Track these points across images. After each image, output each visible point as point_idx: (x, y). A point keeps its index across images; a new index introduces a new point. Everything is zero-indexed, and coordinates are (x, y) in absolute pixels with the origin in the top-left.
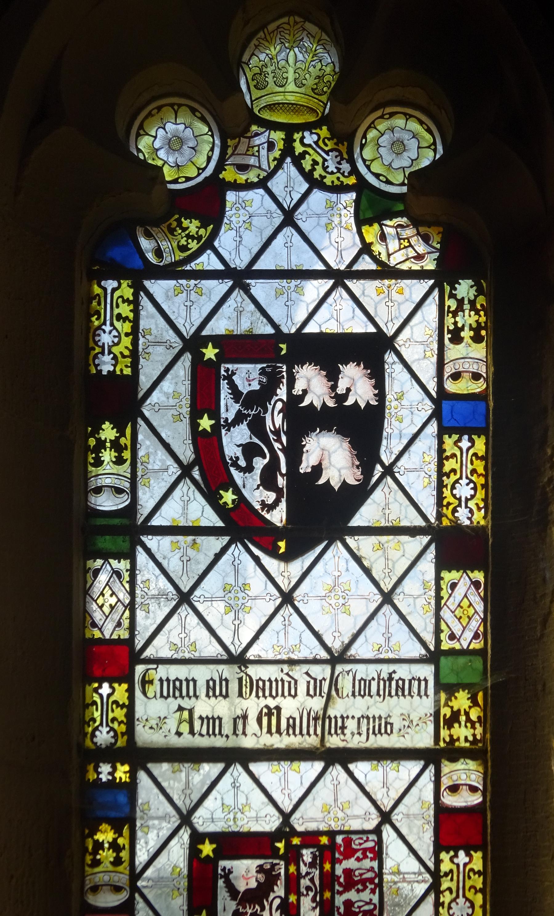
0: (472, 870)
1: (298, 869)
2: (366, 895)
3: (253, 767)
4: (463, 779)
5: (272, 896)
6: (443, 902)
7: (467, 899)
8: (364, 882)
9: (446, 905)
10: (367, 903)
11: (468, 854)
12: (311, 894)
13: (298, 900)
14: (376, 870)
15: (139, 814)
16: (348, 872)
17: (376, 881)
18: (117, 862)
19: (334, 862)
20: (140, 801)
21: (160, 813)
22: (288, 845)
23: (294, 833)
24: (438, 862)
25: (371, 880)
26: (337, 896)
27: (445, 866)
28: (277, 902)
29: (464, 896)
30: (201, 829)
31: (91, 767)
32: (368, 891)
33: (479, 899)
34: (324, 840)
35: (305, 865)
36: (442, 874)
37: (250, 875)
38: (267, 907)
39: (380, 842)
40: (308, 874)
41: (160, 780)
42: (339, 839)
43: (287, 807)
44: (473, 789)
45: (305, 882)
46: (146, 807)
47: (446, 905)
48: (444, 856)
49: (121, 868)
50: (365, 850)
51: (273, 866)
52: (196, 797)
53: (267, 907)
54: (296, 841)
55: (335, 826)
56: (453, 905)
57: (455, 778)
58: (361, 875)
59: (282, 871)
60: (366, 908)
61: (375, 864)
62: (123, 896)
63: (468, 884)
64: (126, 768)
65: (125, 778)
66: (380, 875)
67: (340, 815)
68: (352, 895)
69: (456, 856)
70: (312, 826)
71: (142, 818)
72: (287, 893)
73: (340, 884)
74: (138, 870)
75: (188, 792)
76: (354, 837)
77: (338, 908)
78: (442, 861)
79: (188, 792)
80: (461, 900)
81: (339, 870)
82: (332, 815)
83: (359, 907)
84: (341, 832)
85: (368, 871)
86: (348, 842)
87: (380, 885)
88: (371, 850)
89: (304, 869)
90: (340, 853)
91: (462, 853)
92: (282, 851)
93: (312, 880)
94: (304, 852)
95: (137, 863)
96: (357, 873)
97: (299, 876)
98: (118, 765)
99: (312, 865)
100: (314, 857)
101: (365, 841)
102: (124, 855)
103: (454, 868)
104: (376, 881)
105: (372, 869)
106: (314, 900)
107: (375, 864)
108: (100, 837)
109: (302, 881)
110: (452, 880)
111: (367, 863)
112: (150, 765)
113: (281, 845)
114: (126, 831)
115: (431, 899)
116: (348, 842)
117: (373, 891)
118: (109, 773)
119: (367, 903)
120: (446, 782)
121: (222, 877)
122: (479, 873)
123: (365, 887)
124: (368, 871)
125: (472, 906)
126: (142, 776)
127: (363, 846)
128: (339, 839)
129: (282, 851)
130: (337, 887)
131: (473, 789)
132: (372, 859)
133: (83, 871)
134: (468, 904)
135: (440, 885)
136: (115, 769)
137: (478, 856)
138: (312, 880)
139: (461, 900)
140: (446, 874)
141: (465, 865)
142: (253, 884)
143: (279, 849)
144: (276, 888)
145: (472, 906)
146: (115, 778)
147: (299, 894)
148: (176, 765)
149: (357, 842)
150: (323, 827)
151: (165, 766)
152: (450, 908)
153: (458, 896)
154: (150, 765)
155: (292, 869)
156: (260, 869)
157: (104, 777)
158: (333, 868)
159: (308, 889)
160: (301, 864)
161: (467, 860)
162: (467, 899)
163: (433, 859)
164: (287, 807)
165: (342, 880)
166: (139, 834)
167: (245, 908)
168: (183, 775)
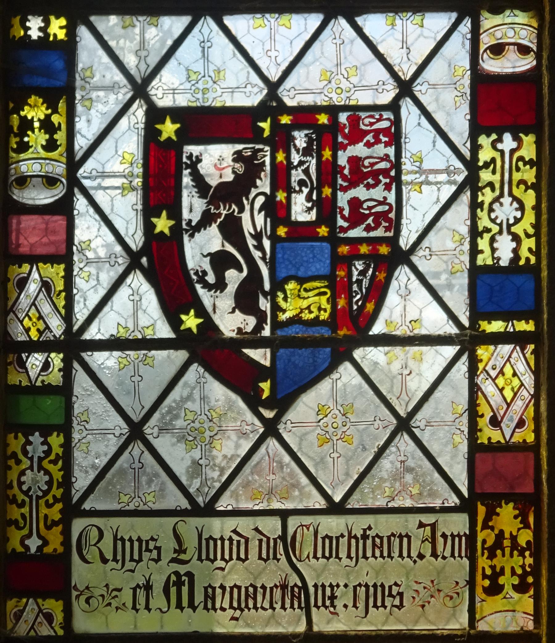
0: (521, 158)
1: (288, 157)
2: (378, 193)
3: (229, 21)
4: (510, 36)
5: (254, 192)
6: (482, 203)
7: (515, 199)
8: (375, 174)
9: (486, 206)
10: (380, 203)
11: (516, 138)
12: (306, 190)
13: (288, 199)
14: (393, 158)
15: (78, 83)
16: (354, 161)
17: (393, 173)
18: (51, 146)
19: (336, 148)
20: (80, 66)
21: (107, 81)
22: (275, 125)
23: (284, 109)
24: (475, 148)
25: (385, 172)
26: (340, 194)
27: (485, 155)
28: (261, 200)
29: (511, 194)
30: (161, 103)
31: (16, 21)
32: (381, 187)
33: (530, 198)
34: (323, 119)
35: (298, 151)
36: (481, 164)
37: (225, 164)
38: (247, 207)
39: (397, 122)
40: (301, 163)
41: (106, 38)
42: (343, 118)
43: (274, 75)
44: (523, 50)
45: (297, 175)
46: (88, 74)
47: (486, 206)
48: (484, 141)
49: (54, 155)
50: (377, 132)
51: (256, 152)
52: (153, 61)
53: (247, 207)
54: (285, 120)
55: (338, 100)
56: (496, 206)
57: (499, 34)
58: (372, 165)
59: (268, 160)
60: (379, 209)
61: (391, 151)
62: (59, 192)
63: (517, 176)
64: (63, 21)
65: (61, 35)
66: (397, 165)
67: (345, 85)
68: (360, 192)
69: (500, 140)
70: (307, 100)
71: (83, 88)
72: (274, 187)
73: (344, 178)
74: (78, 158)
75: (144, 53)
76: (363, 115)
77: (342, 210)
78: (480, 147)
79: (144, 53)
80: (506, 200)
81: (342, 159)
82: (333, 85)
83: (370, 208)
84: (345, 108)
85: (382, 159)
86: (354, 121)
87: (397, 181)
88: (385, 132)
89: (296, 158)
90: (345, 136)
91: (507, 137)
92: (266, 133)
93: (306, 172)
94: (296, 134)
95: (77, 147)
96: (366, 163)
97: (289, 166)
98: (52, 18)
99: (307, 152)
100: (310, 142)
101: (379, 120)
102: (61, 137)
103: (497, 155)
104: (393, 173)
105: (386, 158)
106: (309, 198)
107: (391, 151)
108: (28, 113)
109: (293, 172)
110: (494, 172)
111: (380, 150)
112: (93, 18)
113: (265, 125)
114: (62, 106)
115: (466, 197)
116: (354, 121)
117: (388, 187)
118: (40, 29)
119: (380, 203)
120: (486, 41)
121: (188, 166)
122: (531, 163)
123: (378, 182)
124: (382, 159)
125: (522, 208)
126: (83, 32)
127: (375, 127)
128: (343, 118)
129: (266, 133)
130: (340, 181)
131: (523, 50)
132: (387, 144)
133: (7, 157)
134: (515, 205)
135: (478, 179)
136: (47, 23)
137: (529, 140)
138: (306, 172)
139: (506, 200)
140: (486, 165)
141: (512, 152)
142: (229, 177)
143: (263, 130)
144: (258, 182)
145: (522, 208)
146: (47, 35)
147: (289, 191)
148: (127, 18)
149: (367, 121)
150: (320, 100)
151: (113, 19)
152: (491, 210)
153: (502, 195)
154: (93, 18)
155: (280, 157)
156: (238, 157)
157: (35, 34)
158: (335, 156)
159: (302, 183)
160: (293, 151)
161: (514, 145)
162: (515, 199)
163: (468, 145)
164: (274, 75)
165: (346, 172)
166: (79, 108)
167: (218, 208)
168: (137, 30)
